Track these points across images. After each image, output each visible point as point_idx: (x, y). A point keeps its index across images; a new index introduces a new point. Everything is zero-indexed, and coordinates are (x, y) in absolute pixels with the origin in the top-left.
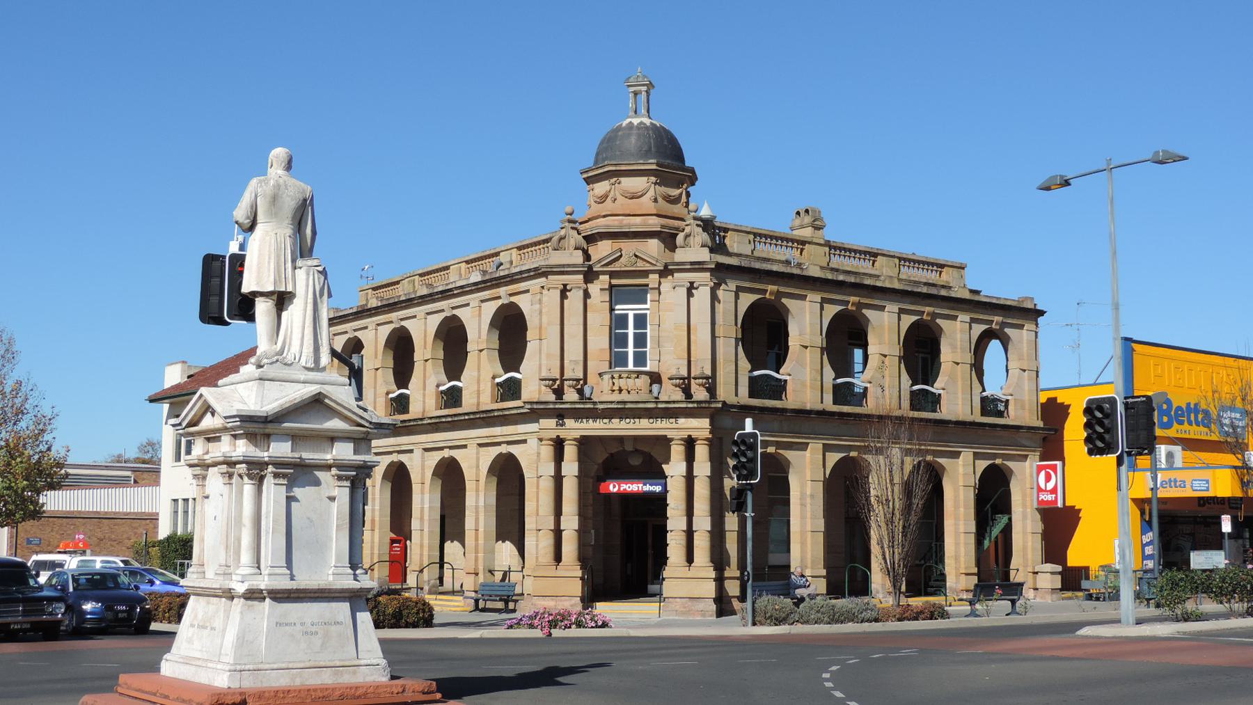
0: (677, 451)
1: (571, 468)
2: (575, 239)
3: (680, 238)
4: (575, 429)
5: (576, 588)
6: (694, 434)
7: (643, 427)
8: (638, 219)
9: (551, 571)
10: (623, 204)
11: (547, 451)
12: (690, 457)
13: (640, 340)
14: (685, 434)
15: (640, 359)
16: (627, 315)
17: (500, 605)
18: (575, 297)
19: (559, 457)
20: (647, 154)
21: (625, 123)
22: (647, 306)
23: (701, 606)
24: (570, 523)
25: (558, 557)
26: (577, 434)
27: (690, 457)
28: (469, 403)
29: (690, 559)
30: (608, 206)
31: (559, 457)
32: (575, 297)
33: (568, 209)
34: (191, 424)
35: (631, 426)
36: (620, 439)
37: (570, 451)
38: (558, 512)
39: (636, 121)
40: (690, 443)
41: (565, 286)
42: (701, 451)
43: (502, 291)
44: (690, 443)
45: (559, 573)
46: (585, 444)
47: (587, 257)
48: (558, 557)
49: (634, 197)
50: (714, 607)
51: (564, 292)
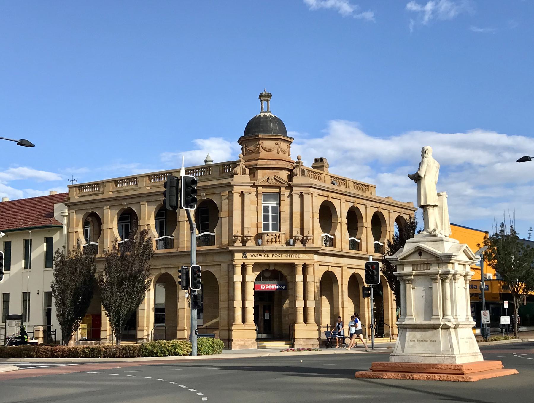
0: (300, 270)
4: (251, 260)
5: (255, 335)
6: (307, 262)
7: (284, 259)
8: (274, 162)
14: (303, 262)
16: (269, 206)
26: (253, 262)
34: (402, 259)
35: (278, 258)
36: (268, 264)
37: (250, 269)
41: (242, 192)
46: (256, 266)
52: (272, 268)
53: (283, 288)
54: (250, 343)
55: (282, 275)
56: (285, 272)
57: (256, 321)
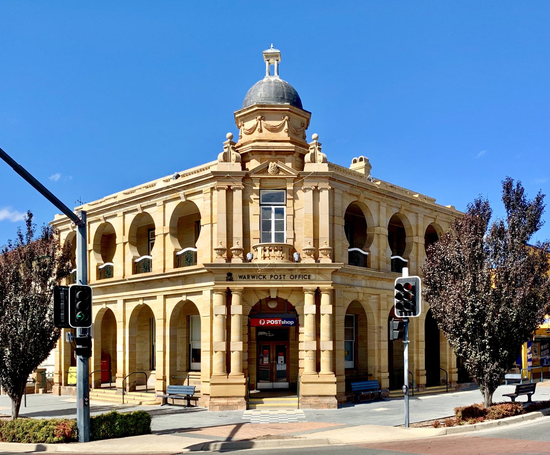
1: (237, 308)
2: (234, 155)
3: (307, 157)
9: (224, 380)
10: (266, 134)
11: (218, 298)
12: (317, 301)
13: (280, 226)
15: (279, 237)
17: (185, 402)
18: (237, 196)
19: (228, 302)
22: (284, 203)
23: (327, 400)
24: (237, 346)
25: (228, 369)
27: (317, 301)
29: (318, 369)
30: (256, 135)
31: (228, 302)
32: (237, 196)
36: (268, 290)
37: (235, 298)
38: (228, 339)
39: (273, 79)
40: (317, 294)
42: (325, 299)
44: (317, 294)
45: (231, 381)
47: (244, 167)
49: (273, 130)
50: (335, 401)
51: (229, 191)
52: (273, 296)
53: (291, 323)
54: (236, 401)
55: (289, 304)
56: (293, 300)
57: (245, 371)
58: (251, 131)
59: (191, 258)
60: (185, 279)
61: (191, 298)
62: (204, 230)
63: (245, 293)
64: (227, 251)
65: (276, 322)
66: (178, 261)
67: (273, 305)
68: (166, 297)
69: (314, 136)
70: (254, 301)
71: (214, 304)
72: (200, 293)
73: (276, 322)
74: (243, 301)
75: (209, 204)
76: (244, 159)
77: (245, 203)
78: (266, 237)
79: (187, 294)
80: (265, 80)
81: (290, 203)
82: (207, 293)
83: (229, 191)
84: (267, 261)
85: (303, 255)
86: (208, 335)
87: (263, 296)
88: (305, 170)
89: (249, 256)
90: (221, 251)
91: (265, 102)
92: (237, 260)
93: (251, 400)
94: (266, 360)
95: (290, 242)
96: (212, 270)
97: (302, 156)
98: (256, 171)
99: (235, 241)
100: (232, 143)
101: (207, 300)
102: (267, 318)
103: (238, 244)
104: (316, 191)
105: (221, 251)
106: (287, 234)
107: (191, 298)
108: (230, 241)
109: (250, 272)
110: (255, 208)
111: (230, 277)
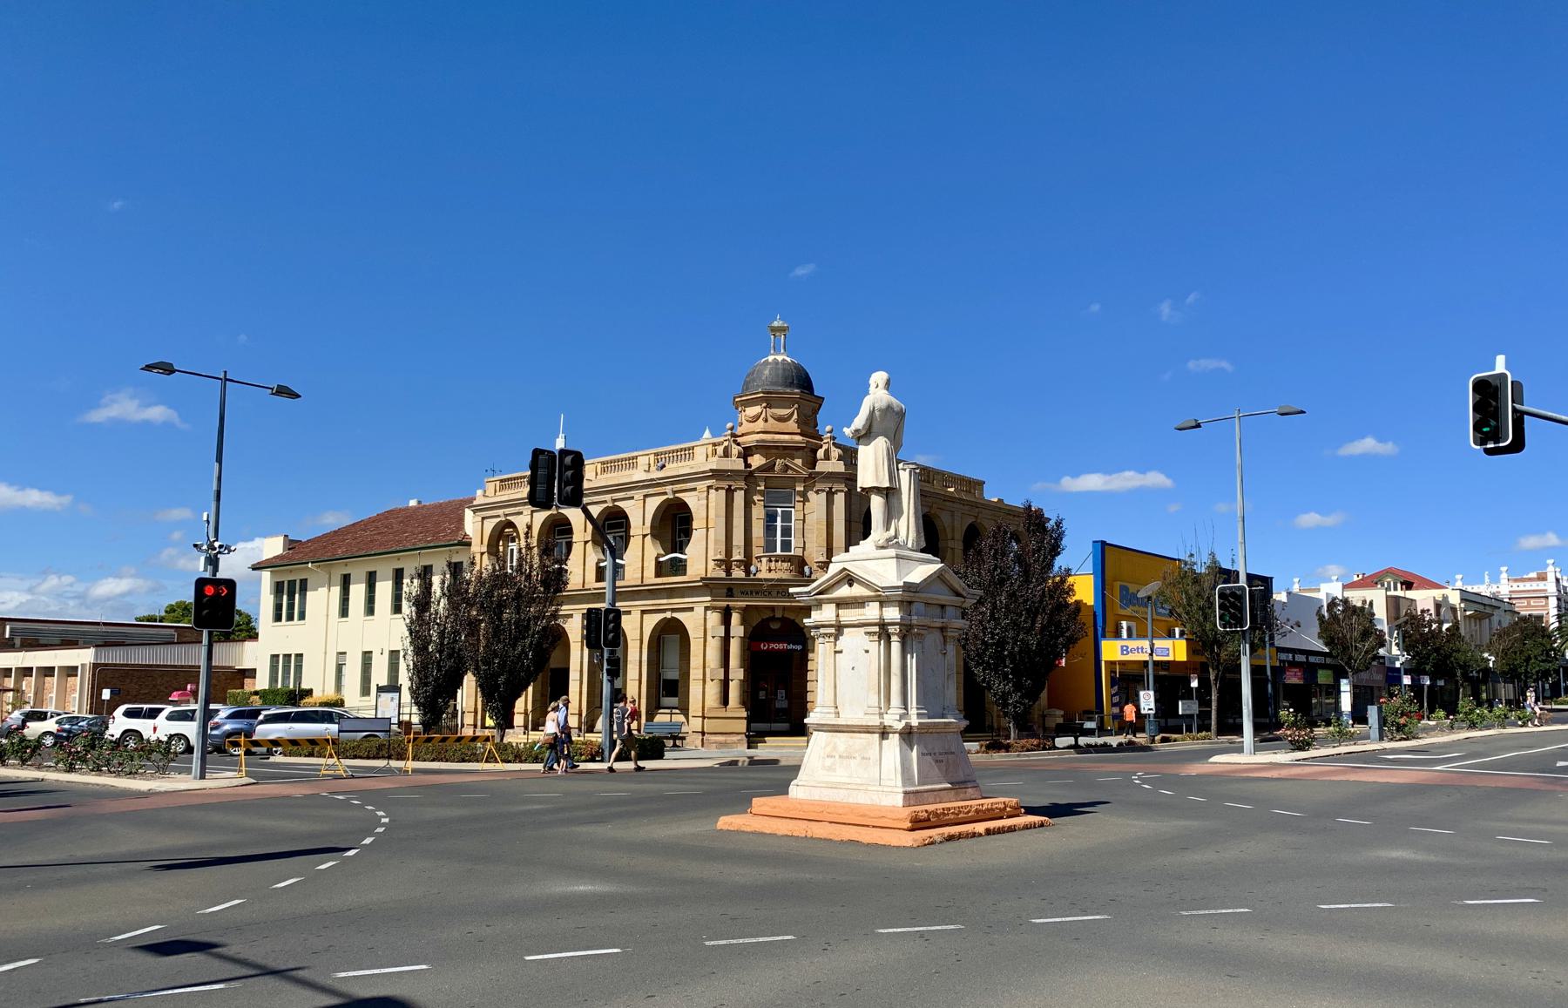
1: (737, 630)
2: (735, 450)
3: (820, 453)
11: (714, 618)
13: (786, 532)
15: (786, 546)
18: (739, 497)
19: (726, 621)
20: (791, 385)
21: (771, 358)
24: (737, 674)
25: (725, 701)
28: (631, 577)
31: (726, 621)
32: (739, 497)
33: (729, 425)
36: (773, 608)
37: (735, 618)
43: (668, 489)
48: (725, 701)
49: (781, 419)
51: (730, 492)
52: (779, 615)
53: (799, 647)
54: (735, 738)
58: (755, 419)
59: (678, 567)
60: (671, 592)
61: (676, 615)
62: (697, 536)
63: (746, 613)
64: (726, 563)
65: (781, 646)
66: (660, 569)
67: (775, 626)
68: (643, 612)
69: (828, 428)
70: (756, 620)
71: (709, 626)
72: (691, 609)
73: (781, 646)
74: (744, 622)
75: (704, 505)
76: (746, 453)
77: (748, 504)
78: (770, 546)
79: (673, 610)
80: (771, 358)
81: (799, 506)
82: (699, 610)
83: (730, 492)
84: (772, 575)
85: (815, 567)
86: (704, 656)
87: (769, 614)
88: (818, 469)
89: (753, 569)
90: (719, 562)
91: (772, 388)
92: (738, 573)
93: (753, 739)
94: (762, 695)
95: (799, 552)
96: (708, 586)
97: (815, 452)
98: (760, 469)
99: (735, 552)
100: (733, 435)
101: (699, 620)
102: (769, 642)
103: (738, 555)
104: (830, 495)
105: (719, 562)
106: (795, 541)
107: (676, 615)
108: (729, 552)
109: (754, 587)
110: (758, 512)
111: (730, 593)
